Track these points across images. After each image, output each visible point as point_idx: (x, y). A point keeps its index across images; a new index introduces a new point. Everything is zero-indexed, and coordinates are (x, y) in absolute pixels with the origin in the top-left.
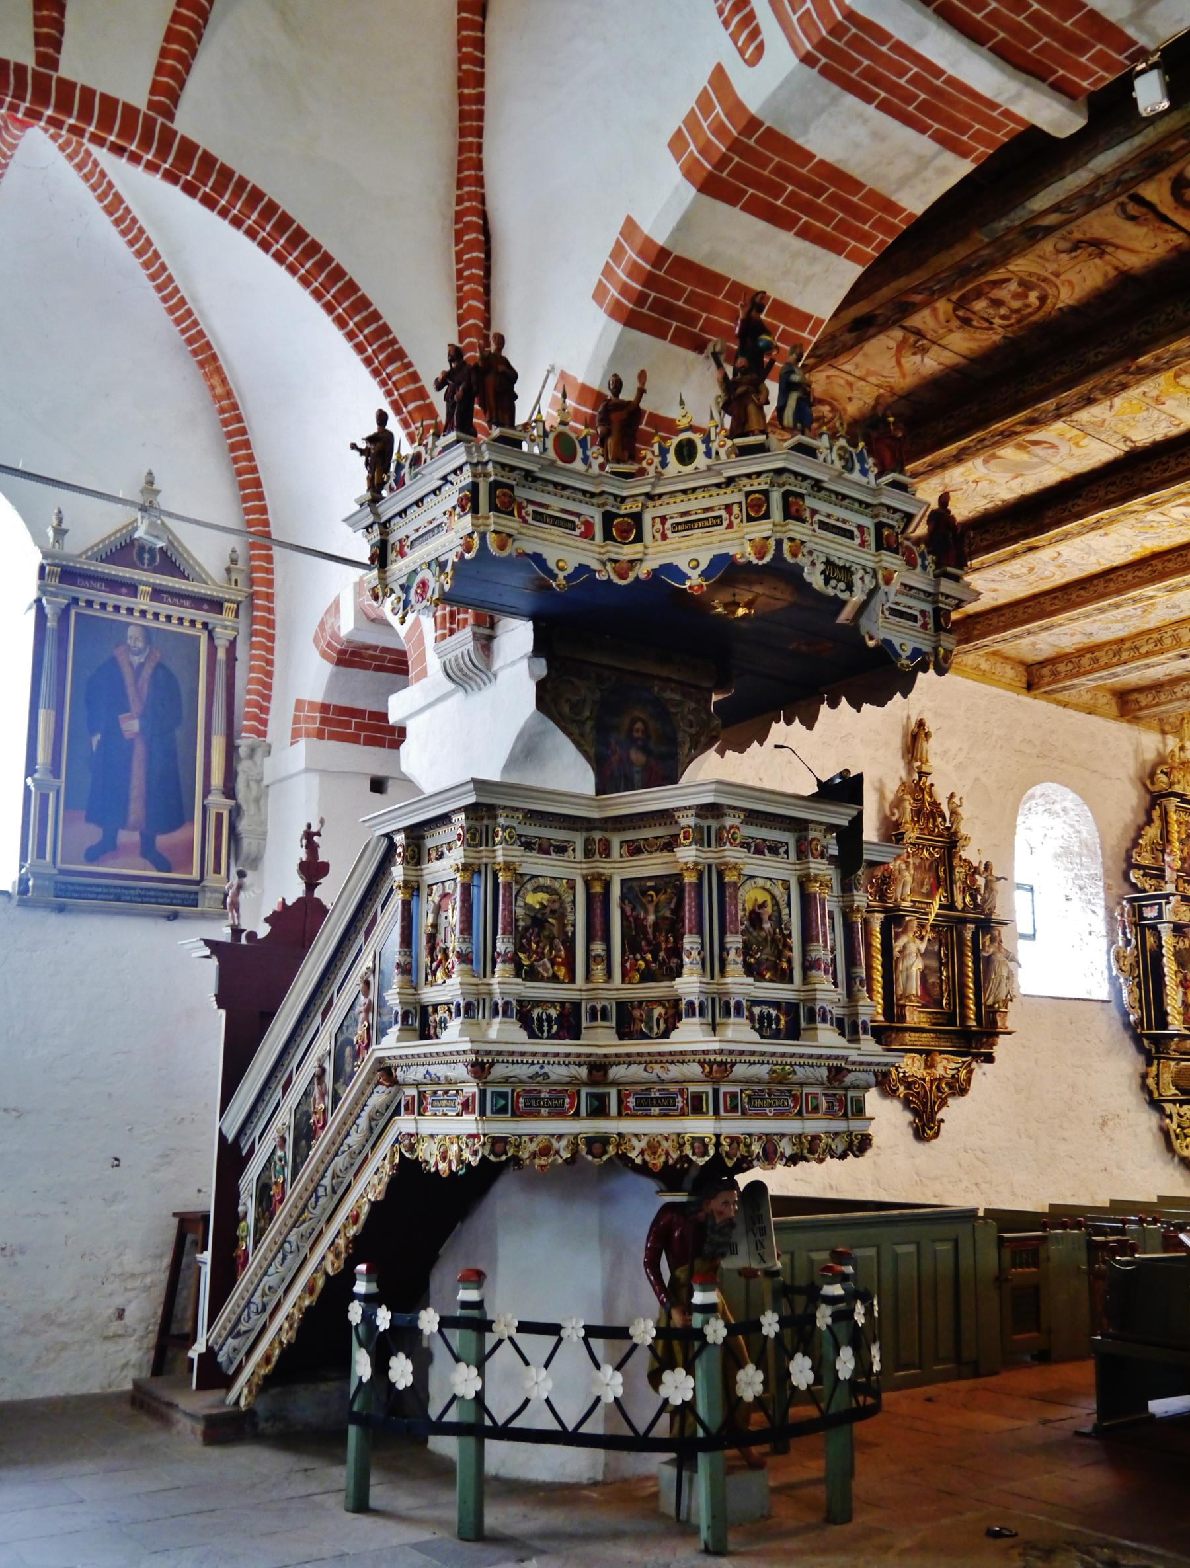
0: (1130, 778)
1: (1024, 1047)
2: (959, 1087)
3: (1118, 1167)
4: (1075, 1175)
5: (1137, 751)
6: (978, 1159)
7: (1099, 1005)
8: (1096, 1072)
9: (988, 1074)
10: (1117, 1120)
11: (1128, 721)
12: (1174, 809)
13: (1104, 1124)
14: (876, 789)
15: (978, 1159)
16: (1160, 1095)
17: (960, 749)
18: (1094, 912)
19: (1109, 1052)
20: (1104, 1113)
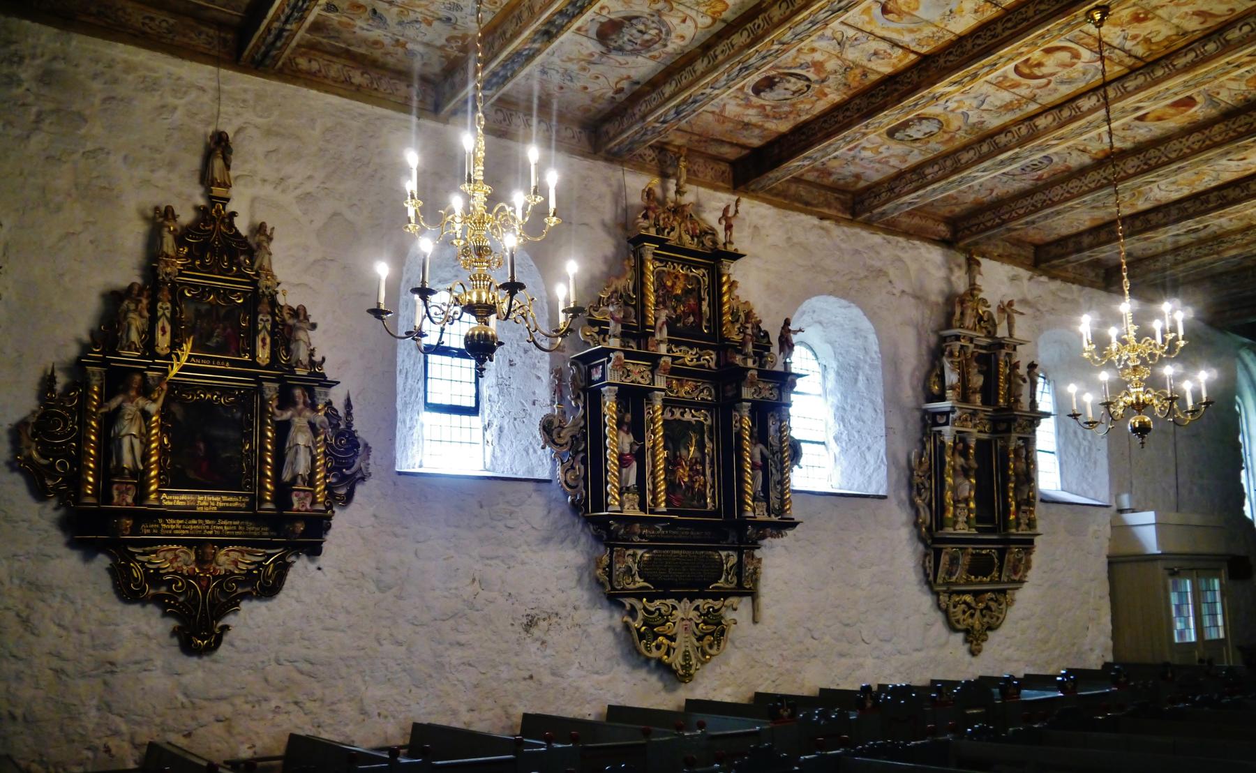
0: (604, 225)
1: (396, 535)
2: (268, 586)
3: (554, 674)
4: (476, 686)
5: (619, 193)
6: (302, 673)
7: (531, 486)
8: (523, 563)
9: (325, 569)
10: (554, 620)
11: (606, 160)
12: (650, 257)
13: (531, 624)
14: (145, 218)
15: (302, 673)
16: (613, 588)
17: (310, 177)
18: (539, 378)
19: (547, 540)
20: (533, 612)
